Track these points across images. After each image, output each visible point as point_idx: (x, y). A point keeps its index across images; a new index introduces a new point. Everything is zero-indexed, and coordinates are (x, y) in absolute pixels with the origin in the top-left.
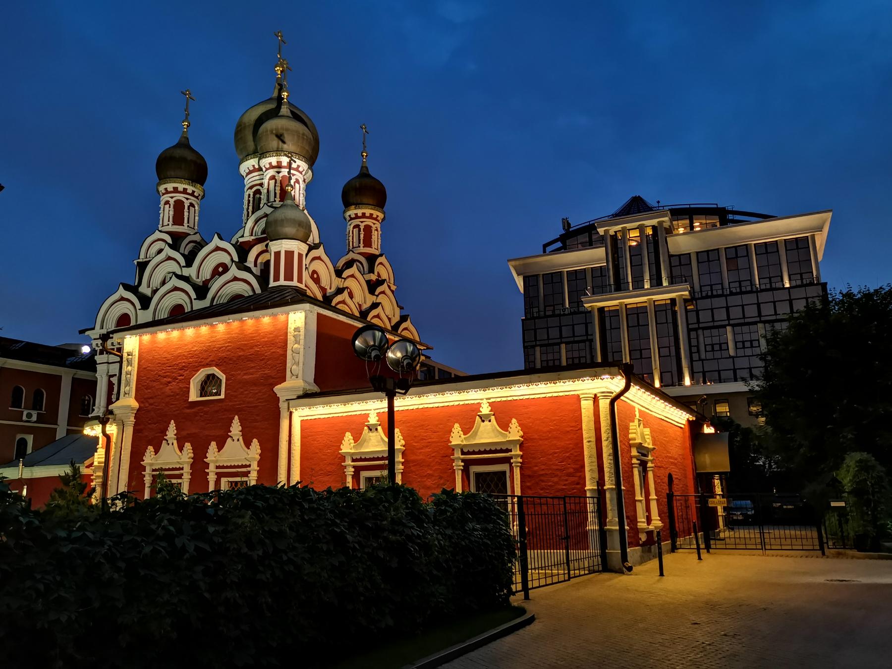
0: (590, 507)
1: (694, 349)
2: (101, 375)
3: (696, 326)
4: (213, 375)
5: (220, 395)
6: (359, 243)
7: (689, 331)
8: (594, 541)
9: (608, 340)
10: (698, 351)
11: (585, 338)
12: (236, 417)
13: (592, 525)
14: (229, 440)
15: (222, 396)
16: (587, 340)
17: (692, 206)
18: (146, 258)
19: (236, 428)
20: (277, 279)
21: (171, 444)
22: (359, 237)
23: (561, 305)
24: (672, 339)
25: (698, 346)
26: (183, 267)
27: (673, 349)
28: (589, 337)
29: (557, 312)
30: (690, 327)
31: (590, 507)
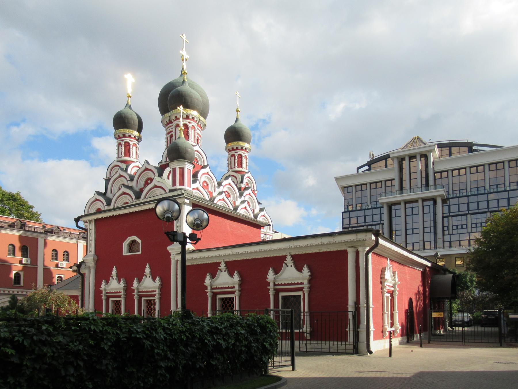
1: (446, 228)
3: (448, 214)
7: (443, 217)
9: (393, 223)
10: (448, 229)
11: (379, 222)
16: (381, 224)
17: (451, 142)
23: (366, 204)
24: (432, 222)
25: (448, 227)
27: (432, 228)
28: (382, 222)
29: (364, 208)
30: (445, 215)
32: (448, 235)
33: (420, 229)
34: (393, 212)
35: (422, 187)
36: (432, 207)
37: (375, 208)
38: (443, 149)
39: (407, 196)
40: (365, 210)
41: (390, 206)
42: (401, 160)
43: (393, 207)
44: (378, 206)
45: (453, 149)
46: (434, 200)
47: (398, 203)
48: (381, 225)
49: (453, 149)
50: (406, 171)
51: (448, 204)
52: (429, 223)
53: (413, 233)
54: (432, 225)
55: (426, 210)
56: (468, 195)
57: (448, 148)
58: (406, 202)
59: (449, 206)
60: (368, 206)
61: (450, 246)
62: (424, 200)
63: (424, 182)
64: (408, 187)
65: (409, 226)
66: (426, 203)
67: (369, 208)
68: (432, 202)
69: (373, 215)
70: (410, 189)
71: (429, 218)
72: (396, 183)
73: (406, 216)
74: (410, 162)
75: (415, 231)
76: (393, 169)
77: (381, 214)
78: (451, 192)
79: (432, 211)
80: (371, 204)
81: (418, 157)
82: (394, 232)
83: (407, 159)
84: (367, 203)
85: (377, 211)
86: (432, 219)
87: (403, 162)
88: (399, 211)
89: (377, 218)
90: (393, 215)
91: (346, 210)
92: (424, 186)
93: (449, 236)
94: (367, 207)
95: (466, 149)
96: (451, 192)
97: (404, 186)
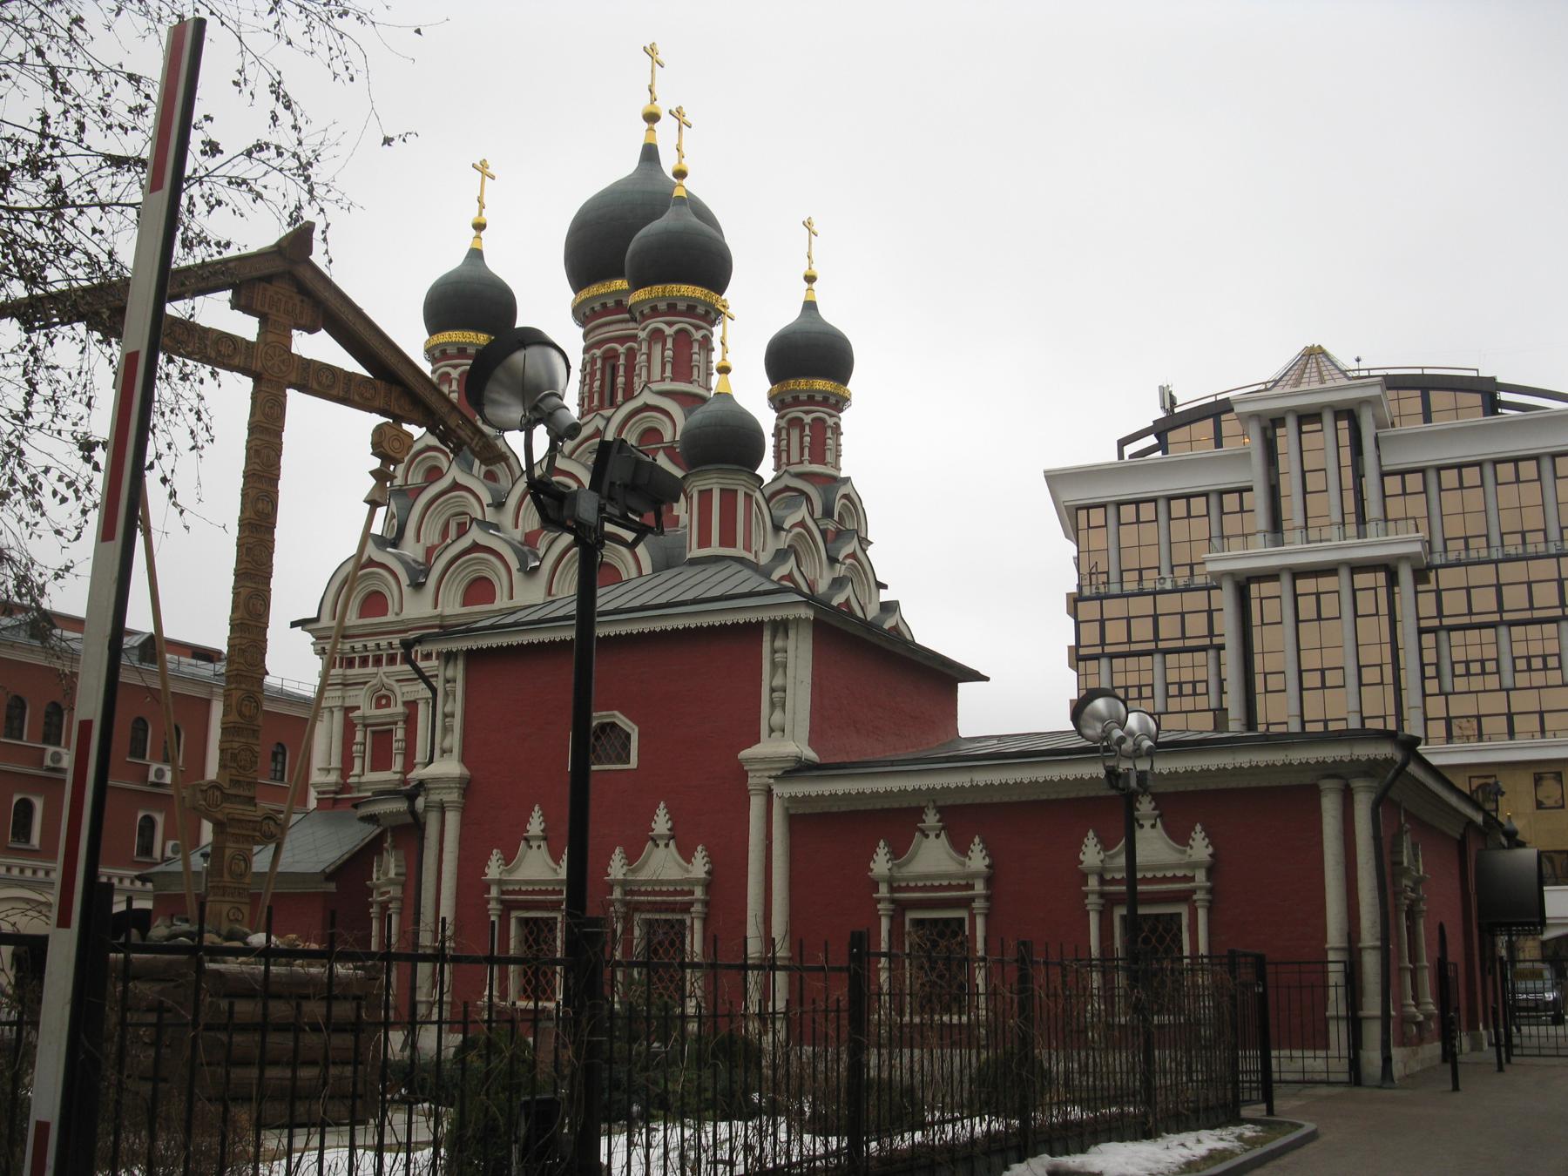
0: (1335, 974)
1: (1430, 671)
2: (330, 708)
3: (1436, 622)
4: (613, 725)
5: (627, 761)
6: (802, 454)
7: (1421, 631)
8: (1338, 1034)
9: (1257, 647)
10: (1438, 676)
11: (1207, 641)
12: (662, 805)
13: (1336, 1003)
14: (650, 843)
15: (634, 763)
16: (1212, 646)
17: (1427, 372)
18: (406, 484)
19: (661, 823)
20: (704, 541)
21: (535, 847)
22: (801, 442)
23: (1156, 570)
24: (1387, 649)
25: (1437, 665)
26: (488, 505)
27: (1388, 670)
28: (1216, 641)
29: (1148, 585)
30: (1424, 624)
31: (1335, 974)
32: (1441, 694)
33: (1347, 671)
34: (1255, 605)
35: (1343, 524)
36: (1383, 593)
37: (1187, 589)
38: (1403, 393)
39: (1295, 552)
40: (1155, 593)
41: (1243, 584)
42: (1271, 424)
43: (1254, 588)
44: (1199, 580)
45: (1435, 396)
46: (1388, 568)
47: (1272, 576)
48: (1212, 653)
49: (1435, 396)
50: (1288, 463)
51: (1433, 586)
52: (1376, 653)
53: (1323, 686)
54: (1388, 658)
55: (1366, 603)
56: (1494, 556)
57: (1418, 393)
58: (1298, 573)
59: (1438, 593)
60: (1164, 579)
61: (1449, 737)
62: (1357, 568)
63: (1350, 505)
64: (1299, 521)
65: (1310, 660)
66: (1362, 580)
67: (1168, 586)
68: (1381, 577)
69: (1183, 614)
70: (1306, 527)
71: (1374, 630)
72: (1258, 500)
73: (1297, 621)
74: (1300, 432)
75: (1332, 678)
76: (1245, 457)
77: (1210, 612)
78: (1438, 546)
79: (1384, 609)
80: (1172, 572)
81: (1328, 418)
82: (1259, 680)
83: (1291, 423)
84: (1159, 568)
85: (1197, 600)
86: (1386, 637)
87: (1279, 431)
88: (1270, 602)
89: (1197, 625)
90: (1256, 619)
91: (1086, 592)
92: (1350, 519)
93: (1443, 697)
94: (1160, 584)
95: (1476, 399)
96: (1438, 546)
97: (1285, 516)
